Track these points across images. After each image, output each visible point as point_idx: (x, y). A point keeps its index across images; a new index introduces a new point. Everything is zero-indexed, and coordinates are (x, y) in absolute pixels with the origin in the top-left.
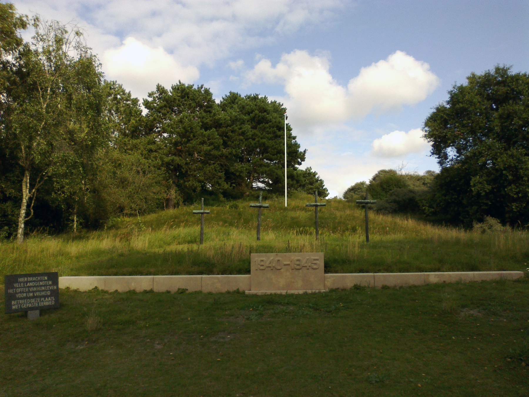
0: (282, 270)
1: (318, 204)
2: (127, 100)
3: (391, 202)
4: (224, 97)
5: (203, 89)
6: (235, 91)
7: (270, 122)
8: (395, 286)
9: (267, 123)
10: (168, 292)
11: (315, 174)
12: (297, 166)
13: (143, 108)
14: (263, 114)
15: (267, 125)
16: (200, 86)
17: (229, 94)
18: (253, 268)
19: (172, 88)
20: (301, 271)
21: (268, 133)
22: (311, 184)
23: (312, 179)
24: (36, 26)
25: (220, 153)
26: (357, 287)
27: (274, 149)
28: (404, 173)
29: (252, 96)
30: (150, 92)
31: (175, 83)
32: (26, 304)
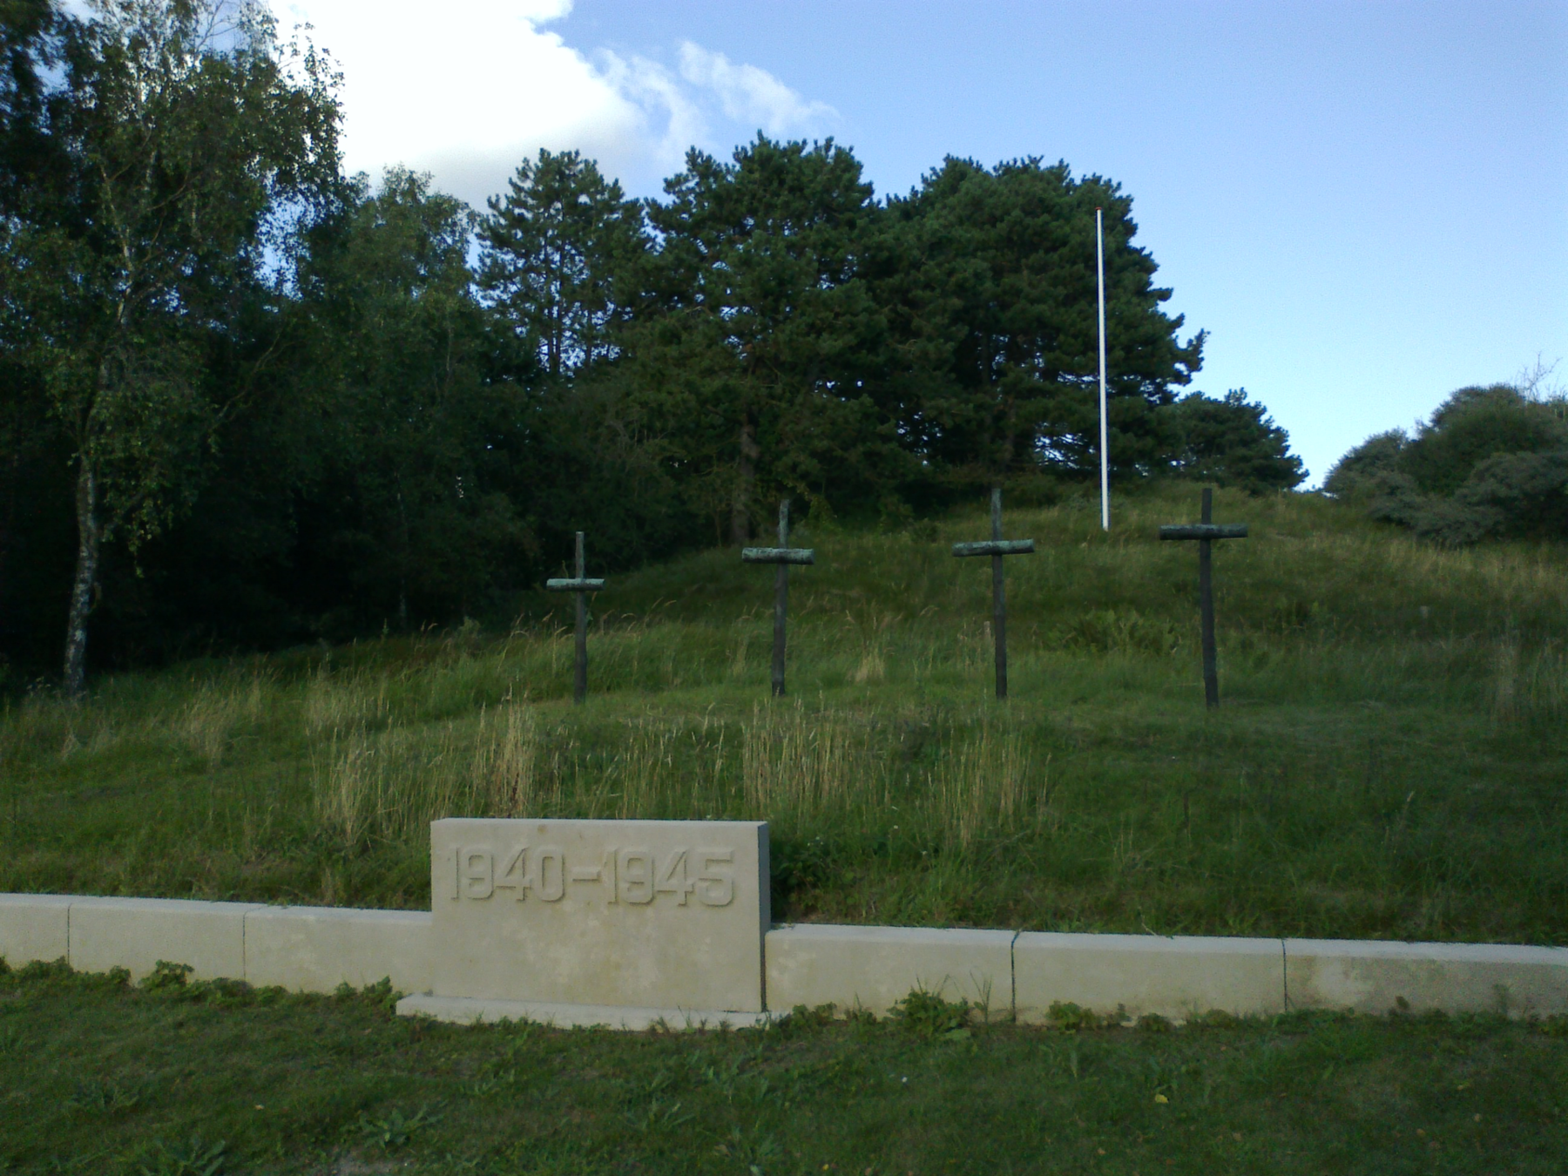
0: (567, 905)
1: (1004, 544)
2: (612, 211)
3: (1479, 504)
4: (928, 173)
5: (832, 152)
6: (962, 154)
7: (1064, 244)
8: (1122, 1013)
9: (1054, 249)
10: (120, 979)
11: (1257, 411)
12: (1173, 387)
13: (649, 229)
14: (1040, 221)
15: (1055, 256)
16: (821, 143)
17: (943, 165)
18: (440, 888)
19: (736, 156)
20: (650, 911)
21: (1055, 281)
22: (1245, 443)
23: (1247, 427)
25: (881, 359)
26: (923, 1012)
27: (1075, 337)
28: (1543, 397)
29: (1019, 164)
30: (671, 176)
31: (747, 140)
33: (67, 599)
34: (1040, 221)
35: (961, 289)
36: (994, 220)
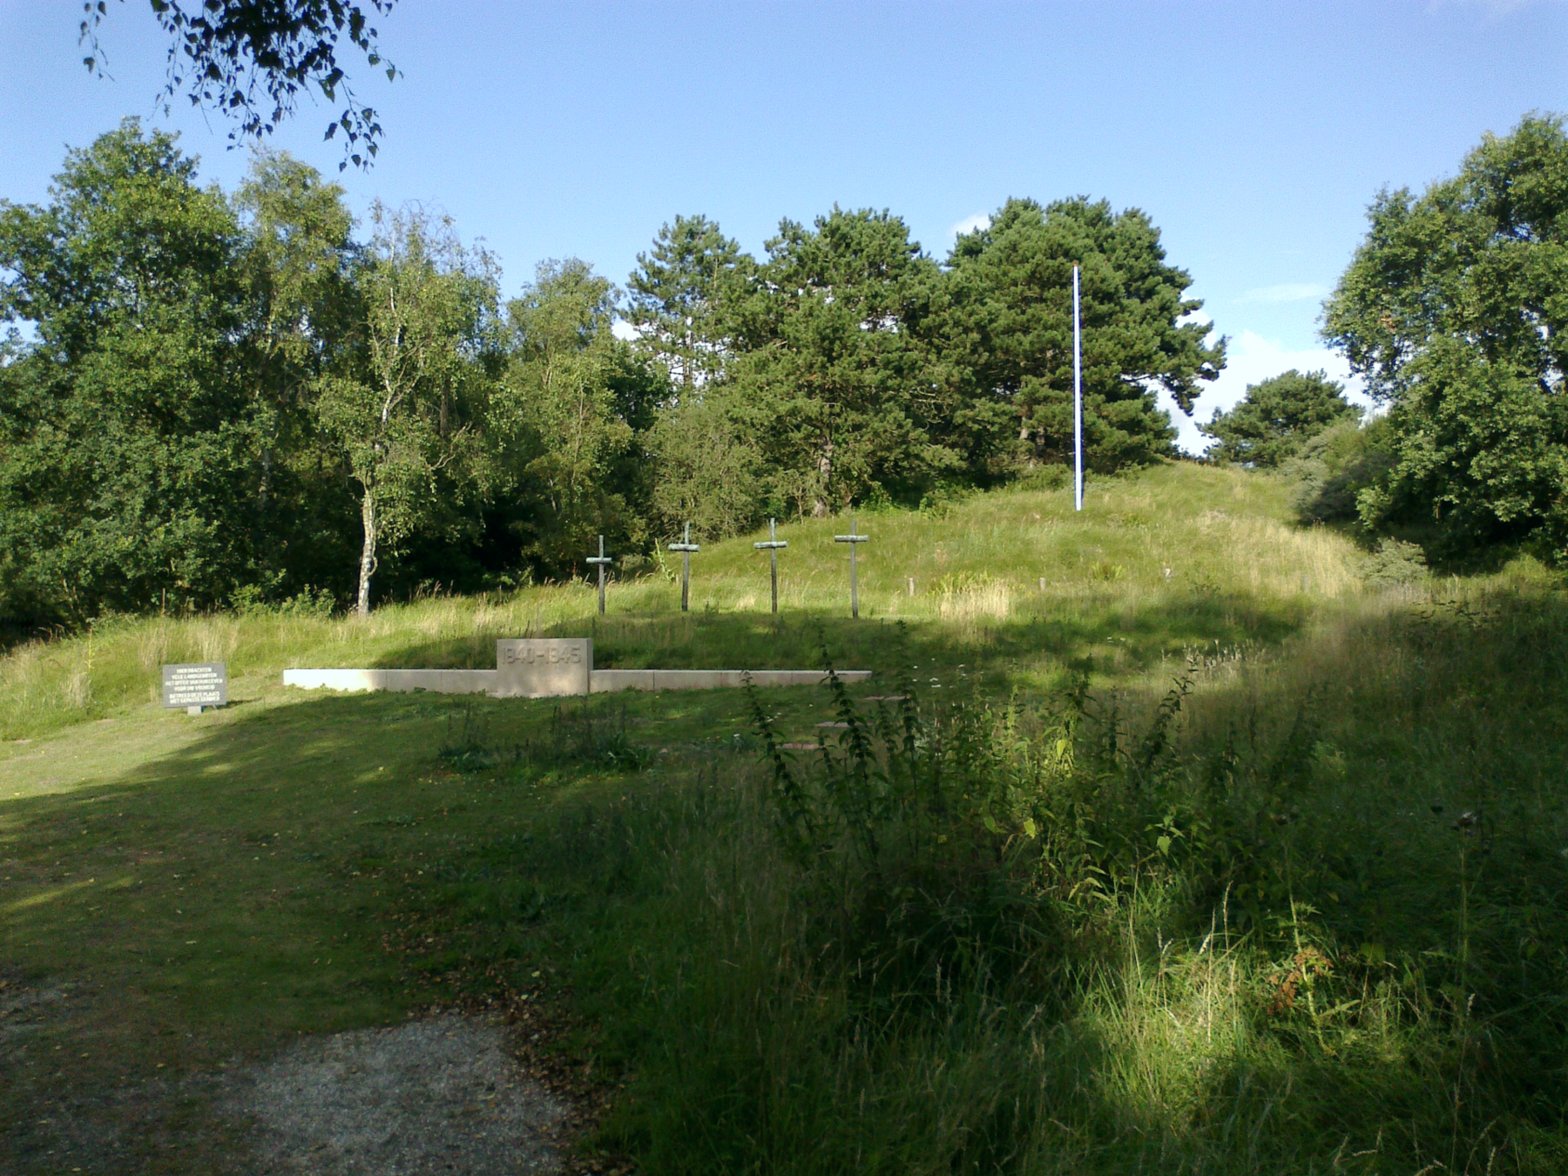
1: (774, 544)
24: (378, 219)
32: (185, 699)
33: (358, 568)
34: (1056, 263)
35: (980, 327)
36: (1025, 260)
